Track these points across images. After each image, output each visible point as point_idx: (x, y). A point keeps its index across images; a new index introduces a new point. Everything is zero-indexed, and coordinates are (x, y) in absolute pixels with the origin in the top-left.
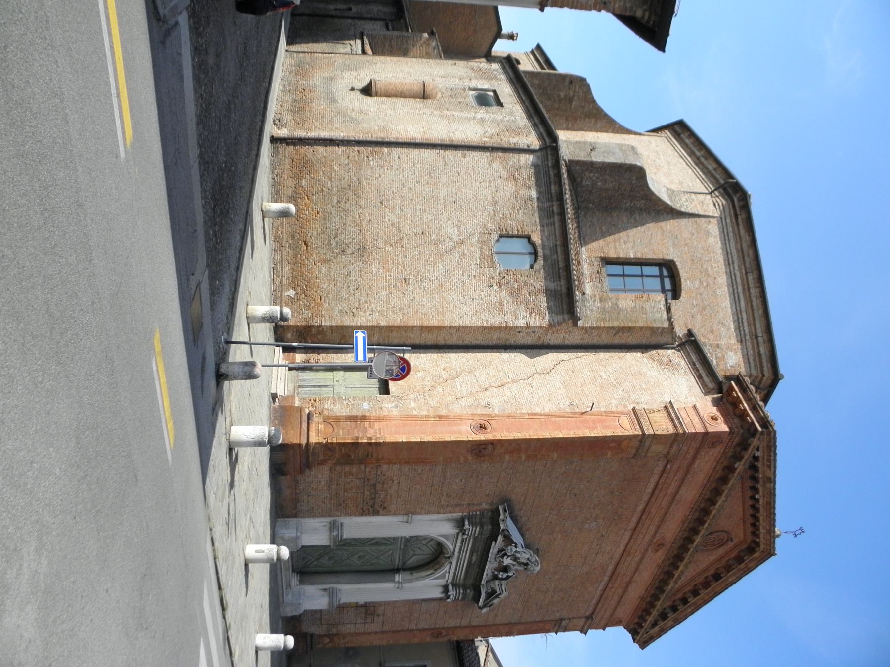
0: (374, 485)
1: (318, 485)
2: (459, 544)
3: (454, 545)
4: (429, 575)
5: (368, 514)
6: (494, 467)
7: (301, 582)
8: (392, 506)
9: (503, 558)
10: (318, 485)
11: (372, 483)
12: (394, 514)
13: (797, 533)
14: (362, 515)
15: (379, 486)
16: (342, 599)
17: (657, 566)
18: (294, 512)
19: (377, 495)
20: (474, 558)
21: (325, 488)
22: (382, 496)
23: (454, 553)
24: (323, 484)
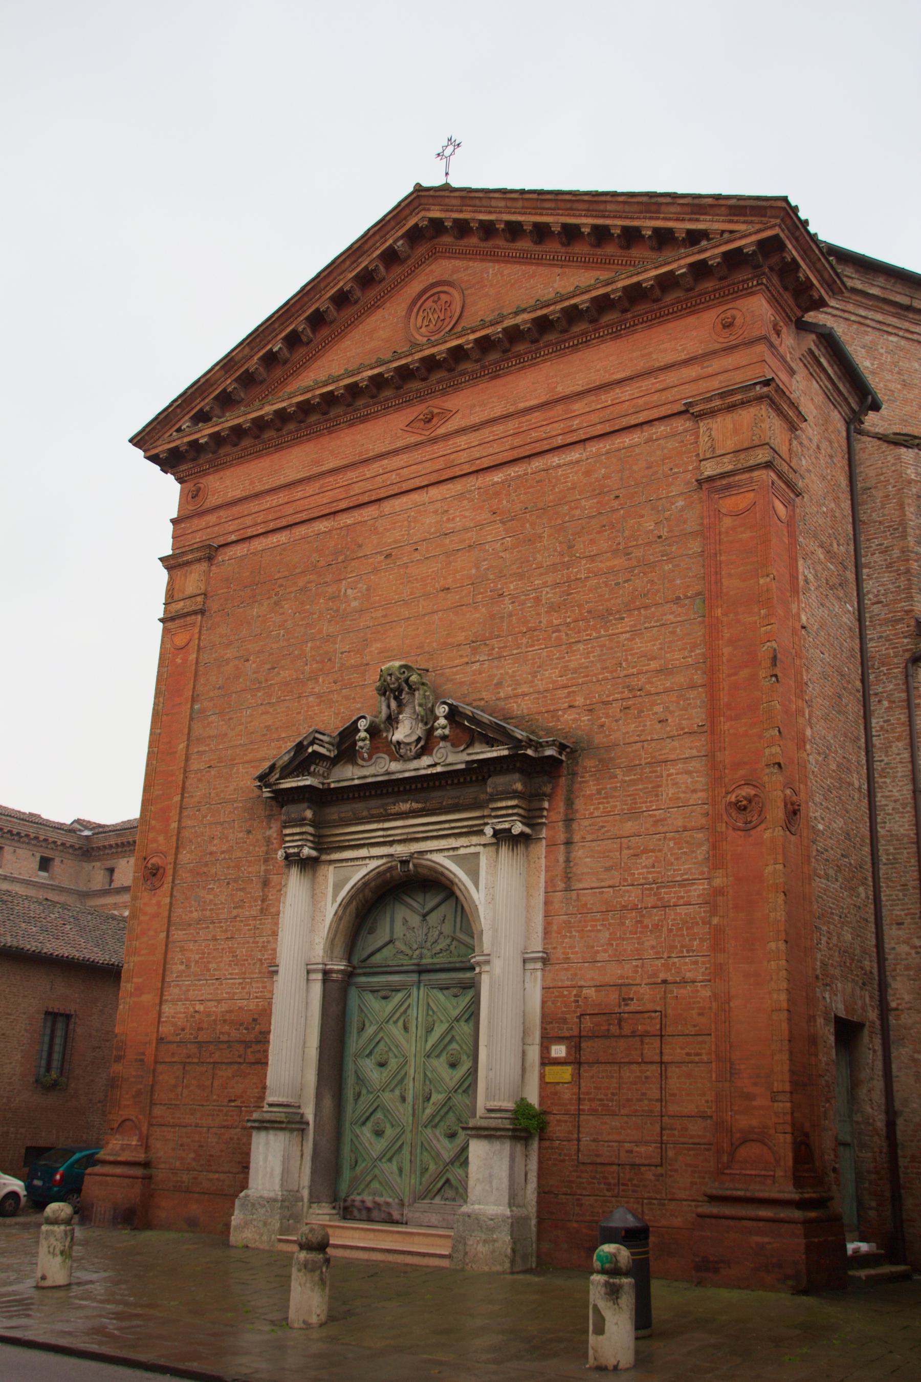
2: (363, 852)
3: (367, 861)
6: (191, 841)
13: (451, 148)
15: (202, 1037)
17: (498, 377)
19: (223, 1038)
20: (405, 807)
22: (227, 1028)
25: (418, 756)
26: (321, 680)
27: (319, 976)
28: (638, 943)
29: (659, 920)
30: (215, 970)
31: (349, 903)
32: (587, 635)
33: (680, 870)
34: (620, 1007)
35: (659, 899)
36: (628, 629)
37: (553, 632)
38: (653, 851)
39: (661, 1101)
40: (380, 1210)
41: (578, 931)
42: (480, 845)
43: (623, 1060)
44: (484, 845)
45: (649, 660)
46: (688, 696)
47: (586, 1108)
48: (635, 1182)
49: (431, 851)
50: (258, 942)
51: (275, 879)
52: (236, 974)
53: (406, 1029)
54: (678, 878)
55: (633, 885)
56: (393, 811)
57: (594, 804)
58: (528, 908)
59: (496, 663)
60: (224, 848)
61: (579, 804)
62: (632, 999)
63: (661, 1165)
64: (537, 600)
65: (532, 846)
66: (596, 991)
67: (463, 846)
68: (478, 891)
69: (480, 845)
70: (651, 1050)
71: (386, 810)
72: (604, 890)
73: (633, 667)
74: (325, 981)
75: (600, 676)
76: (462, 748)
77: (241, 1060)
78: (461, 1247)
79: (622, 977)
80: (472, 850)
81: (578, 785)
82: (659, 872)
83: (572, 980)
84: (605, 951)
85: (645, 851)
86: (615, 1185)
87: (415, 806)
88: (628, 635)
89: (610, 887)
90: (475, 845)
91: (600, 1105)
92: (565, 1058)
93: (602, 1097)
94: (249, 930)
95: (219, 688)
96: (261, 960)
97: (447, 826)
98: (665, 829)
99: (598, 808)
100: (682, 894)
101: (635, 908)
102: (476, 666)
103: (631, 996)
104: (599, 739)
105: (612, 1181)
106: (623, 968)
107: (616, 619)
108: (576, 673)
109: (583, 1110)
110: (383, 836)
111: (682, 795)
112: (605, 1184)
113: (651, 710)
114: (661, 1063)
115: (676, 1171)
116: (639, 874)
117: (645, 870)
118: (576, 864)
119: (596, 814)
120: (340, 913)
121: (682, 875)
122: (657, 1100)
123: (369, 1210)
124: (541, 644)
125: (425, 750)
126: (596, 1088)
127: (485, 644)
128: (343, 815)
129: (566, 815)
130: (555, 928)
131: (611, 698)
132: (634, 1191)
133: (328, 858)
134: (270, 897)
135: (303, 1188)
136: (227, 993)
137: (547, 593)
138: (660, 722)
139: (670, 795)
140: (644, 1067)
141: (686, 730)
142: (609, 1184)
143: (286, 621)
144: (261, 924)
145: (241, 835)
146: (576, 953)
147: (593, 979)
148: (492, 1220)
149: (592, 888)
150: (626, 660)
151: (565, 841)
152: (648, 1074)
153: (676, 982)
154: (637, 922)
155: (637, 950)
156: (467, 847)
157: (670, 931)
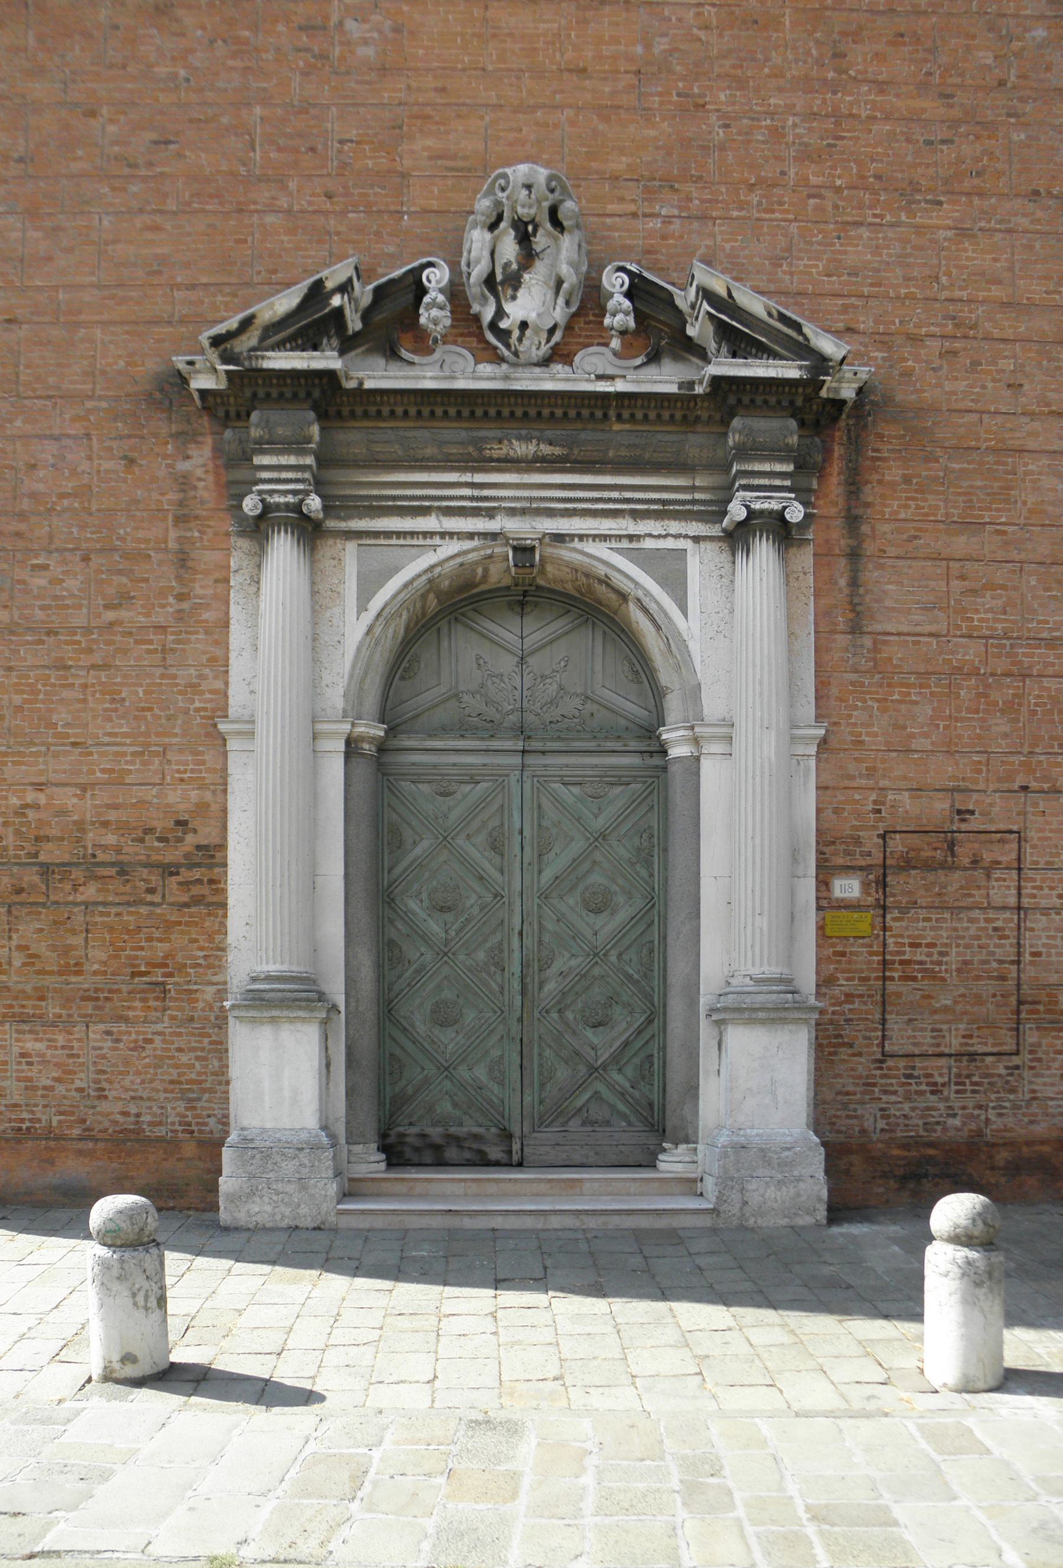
0: (46, 870)
1: (44, 1062)
2: (430, 523)
3: (437, 540)
4: (653, 621)
5: (217, 885)
7: (687, 1137)
8: (173, 797)
9: (508, 333)
10: (44, 1062)
11: (36, 879)
12: (223, 787)
14: (224, 905)
15: (49, 853)
16: (755, 971)
18: (189, 1150)
21: (61, 1039)
22: (111, 839)
23: (494, 536)
24: (31, 1045)
25: (545, 362)
26: (292, 185)
27: (341, 746)
28: (981, 728)
29: (1015, 695)
30: (67, 725)
31: (398, 614)
32: (875, 216)
33: (1048, 623)
34: (952, 822)
35: (1014, 664)
36: (949, 222)
37: (810, 196)
38: (1003, 587)
39: (1018, 962)
40: (461, 1147)
41: (878, 700)
42: (686, 536)
43: (956, 904)
44: (696, 539)
45: (988, 282)
46: (1054, 354)
47: (896, 975)
48: (975, 1079)
49: (581, 537)
50: (175, 677)
51: (209, 557)
52: (125, 735)
53: (496, 846)
54: (1045, 635)
55: (970, 637)
56: (495, 454)
57: (899, 499)
58: (792, 654)
59: (696, 225)
60: (69, 486)
61: (869, 493)
62: (972, 812)
63: (1017, 1053)
64: (777, 133)
65: (793, 551)
66: (911, 797)
67: (650, 535)
68: (686, 617)
69: (686, 536)
70: (1003, 891)
71: (481, 450)
72: (921, 639)
73: (961, 289)
74: (348, 755)
75: (903, 291)
76: (638, 361)
77: (157, 898)
78: (735, 1197)
79: (955, 778)
80: (670, 544)
81: (868, 463)
82: (1014, 622)
83: (868, 776)
84: (926, 735)
85: (990, 586)
86: (943, 1085)
87: (546, 449)
88: (949, 234)
89: (931, 635)
90: (676, 537)
91: (919, 971)
92: (859, 900)
93: (924, 958)
94: (148, 652)
95: (21, 160)
96: (186, 712)
97: (615, 495)
98: (1023, 556)
99: (906, 506)
100: (1051, 659)
101: (975, 672)
102: (655, 224)
103: (971, 807)
104: (903, 395)
105: (940, 1080)
106: (957, 764)
107: (927, 202)
108: (856, 275)
109: (892, 979)
110: (472, 498)
111: (1050, 508)
112: (928, 1084)
113: (996, 364)
114: (1019, 908)
115: (1039, 1060)
116: (979, 620)
117: (990, 616)
118: (867, 592)
119: (902, 516)
120: (378, 630)
121: (1051, 630)
122: (1012, 962)
123: (437, 1148)
124: (787, 212)
125: (560, 355)
126: (911, 945)
127: (672, 187)
128: (378, 448)
129: (849, 510)
130: (834, 691)
131: (924, 331)
132: (974, 1092)
133: (343, 525)
134: (199, 591)
135: (337, 1119)
136: (103, 771)
137: (795, 125)
138: (1009, 386)
139: (1029, 505)
140: (991, 915)
141: (1054, 408)
142: (935, 1084)
143: (191, 51)
144: (178, 642)
145: (110, 465)
146: (876, 735)
147: (905, 778)
148: (788, 1149)
149: (899, 634)
150: (948, 274)
151: (848, 551)
152: (999, 924)
153: (1042, 791)
154: (979, 695)
155: (979, 737)
156: (659, 536)
157: (1034, 713)
